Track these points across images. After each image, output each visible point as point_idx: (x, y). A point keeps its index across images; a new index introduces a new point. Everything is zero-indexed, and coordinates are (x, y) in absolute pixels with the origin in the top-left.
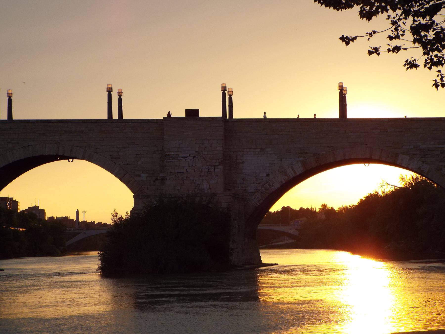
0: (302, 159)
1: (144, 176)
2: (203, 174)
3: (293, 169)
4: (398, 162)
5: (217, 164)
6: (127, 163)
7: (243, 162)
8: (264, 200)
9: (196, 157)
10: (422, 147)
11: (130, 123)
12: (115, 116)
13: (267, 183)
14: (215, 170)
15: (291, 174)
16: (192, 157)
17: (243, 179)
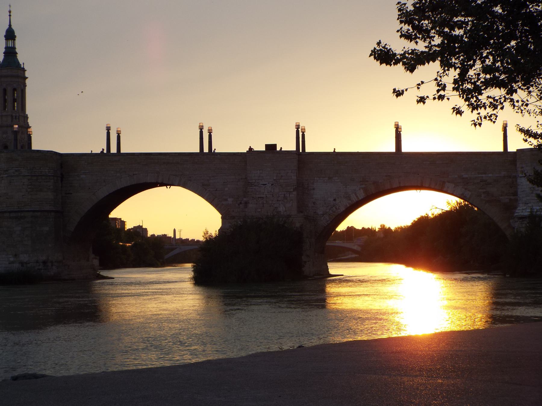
0: (363, 186)
1: (230, 200)
2: (279, 200)
3: (356, 195)
4: (445, 189)
5: (292, 190)
6: (216, 189)
7: (314, 189)
8: (331, 220)
9: (274, 184)
11: (219, 156)
12: (206, 150)
13: (334, 206)
14: (291, 196)
15: (354, 199)
16: (271, 185)
17: (314, 203)
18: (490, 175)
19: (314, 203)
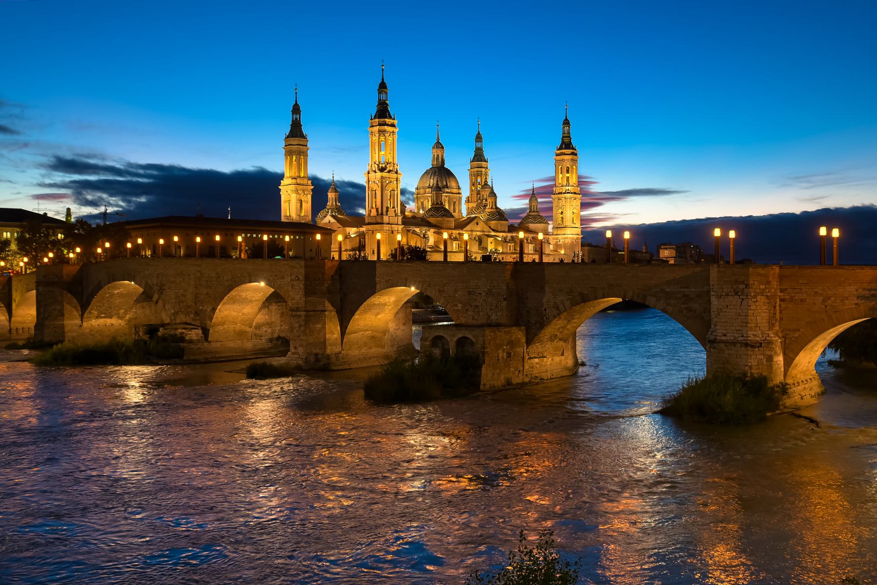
1: (460, 306)
5: (502, 300)
7: (528, 298)
10: (668, 290)
14: (502, 305)
18: (693, 290)
19: (528, 312)
